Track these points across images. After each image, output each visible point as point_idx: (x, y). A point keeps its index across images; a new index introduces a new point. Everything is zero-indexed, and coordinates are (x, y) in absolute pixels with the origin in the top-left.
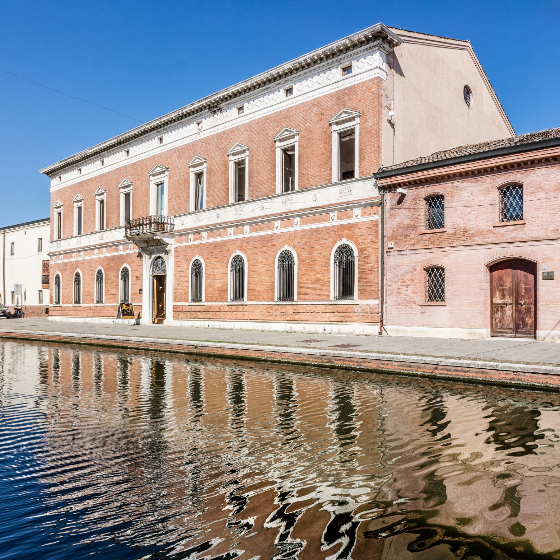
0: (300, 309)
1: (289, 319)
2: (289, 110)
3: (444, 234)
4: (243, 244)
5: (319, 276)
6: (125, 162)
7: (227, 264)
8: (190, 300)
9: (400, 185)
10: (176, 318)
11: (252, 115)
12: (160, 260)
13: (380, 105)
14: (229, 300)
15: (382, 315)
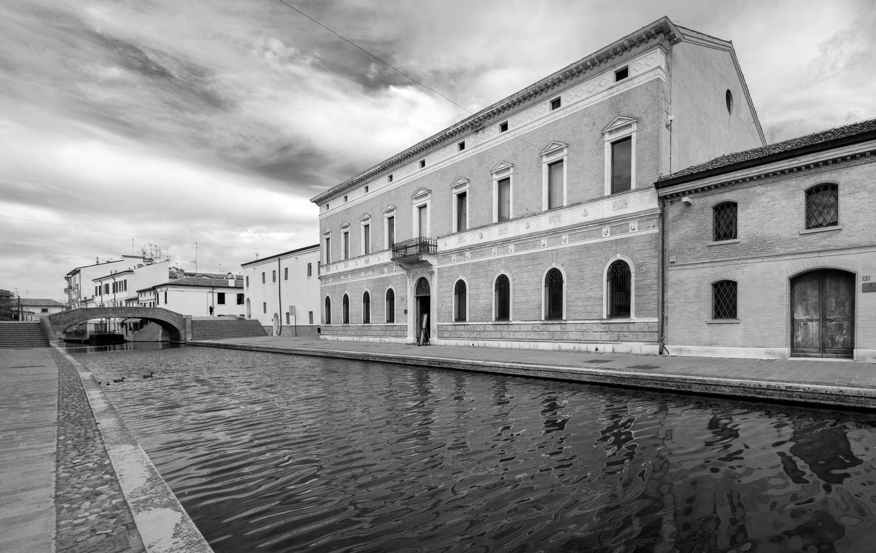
9: (684, 194)
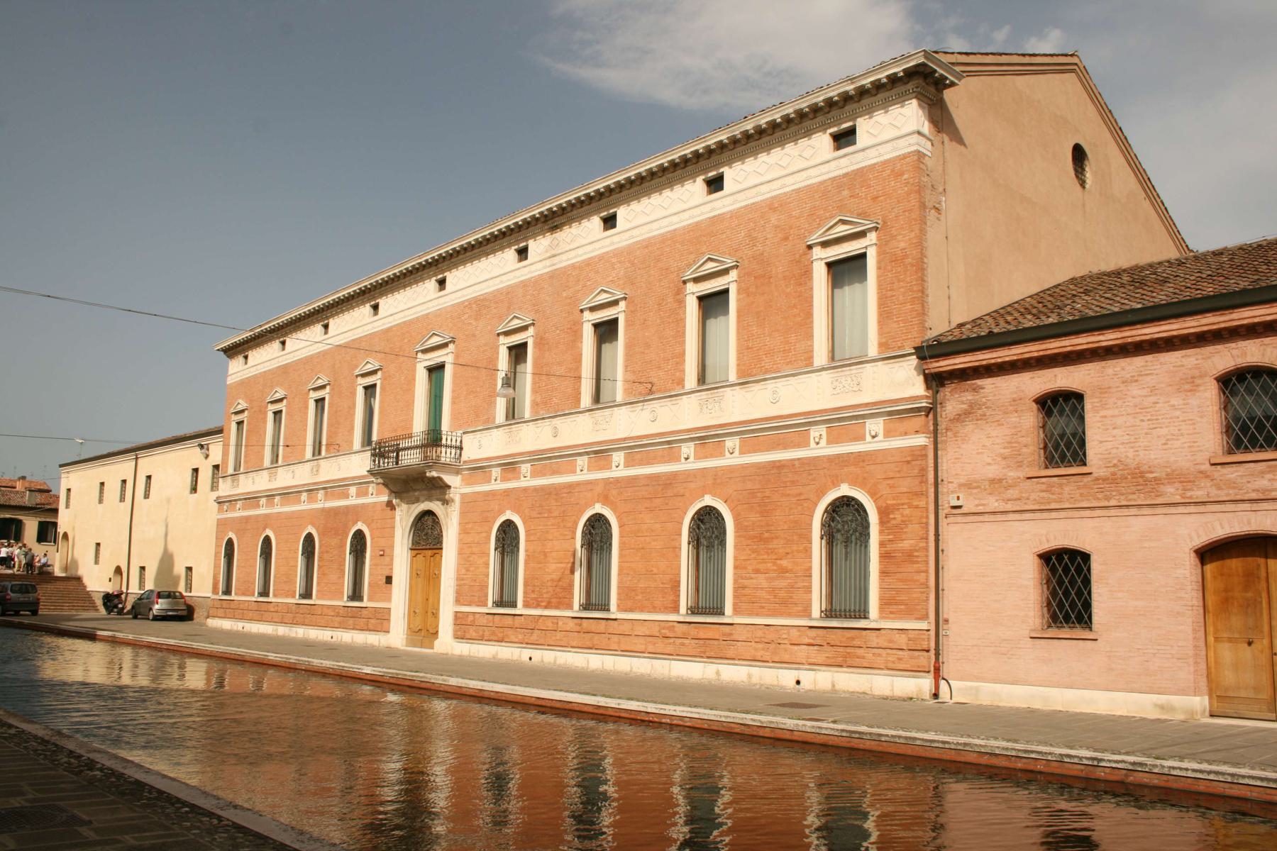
0: (739, 634)
1: (712, 654)
2: (715, 220)
3: (1086, 479)
4: (608, 490)
5: (784, 563)
6: (370, 327)
7: (574, 533)
8: (490, 603)
10: (460, 636)
11: (635, 232)
12: (429, 520)
13: (923, 206)
14: (576, 606)
15: (937, 654)
